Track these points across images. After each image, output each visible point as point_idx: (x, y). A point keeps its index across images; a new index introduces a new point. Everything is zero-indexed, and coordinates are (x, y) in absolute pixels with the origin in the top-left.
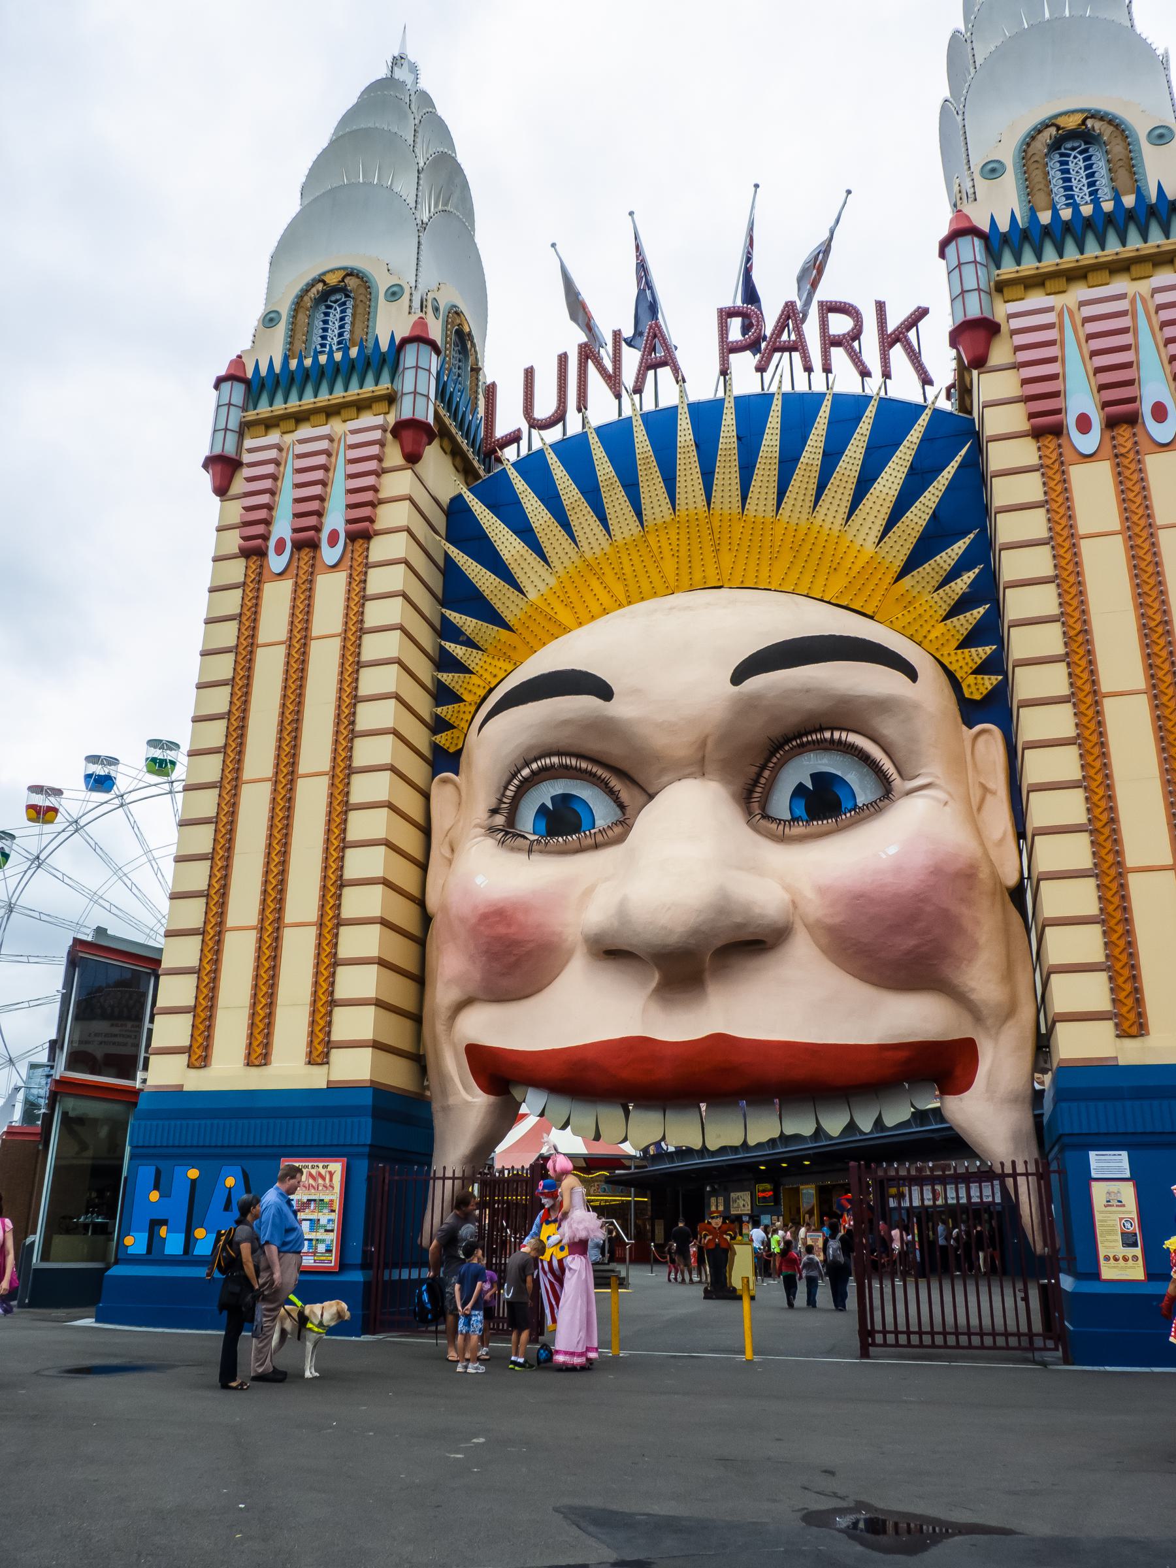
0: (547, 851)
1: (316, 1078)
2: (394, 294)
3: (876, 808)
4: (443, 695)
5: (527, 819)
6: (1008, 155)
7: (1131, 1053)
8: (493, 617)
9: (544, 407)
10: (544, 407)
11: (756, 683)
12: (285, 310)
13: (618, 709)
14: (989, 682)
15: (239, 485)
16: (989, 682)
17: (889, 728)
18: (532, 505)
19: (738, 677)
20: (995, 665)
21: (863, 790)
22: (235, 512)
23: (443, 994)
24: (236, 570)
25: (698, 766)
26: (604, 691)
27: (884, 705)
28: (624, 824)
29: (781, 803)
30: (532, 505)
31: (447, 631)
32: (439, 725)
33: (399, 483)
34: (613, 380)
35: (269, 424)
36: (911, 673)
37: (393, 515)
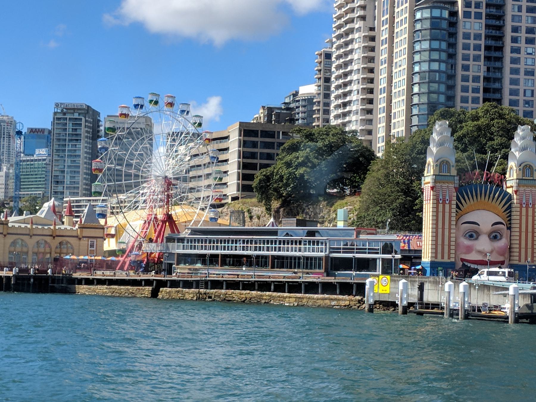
0: (470, 240)
1: (449, 261)
3: (500, 239)
5: (467, 235)
7: (520, 263)
11: (494, 226)
12: (438, 164)
14: (510, 225)
16: (510, 225)
17: (502, 231)
18: (466, 196)
19: (492, 225)
20: (510, 224)
22: (435, 193)
23: (458, 253)
24: (435, 201)
25: (486, 234)
26: (479, 225)
27: (503, 229)
29: (491, 237)
30: (466, 196)
36: (505, 225)
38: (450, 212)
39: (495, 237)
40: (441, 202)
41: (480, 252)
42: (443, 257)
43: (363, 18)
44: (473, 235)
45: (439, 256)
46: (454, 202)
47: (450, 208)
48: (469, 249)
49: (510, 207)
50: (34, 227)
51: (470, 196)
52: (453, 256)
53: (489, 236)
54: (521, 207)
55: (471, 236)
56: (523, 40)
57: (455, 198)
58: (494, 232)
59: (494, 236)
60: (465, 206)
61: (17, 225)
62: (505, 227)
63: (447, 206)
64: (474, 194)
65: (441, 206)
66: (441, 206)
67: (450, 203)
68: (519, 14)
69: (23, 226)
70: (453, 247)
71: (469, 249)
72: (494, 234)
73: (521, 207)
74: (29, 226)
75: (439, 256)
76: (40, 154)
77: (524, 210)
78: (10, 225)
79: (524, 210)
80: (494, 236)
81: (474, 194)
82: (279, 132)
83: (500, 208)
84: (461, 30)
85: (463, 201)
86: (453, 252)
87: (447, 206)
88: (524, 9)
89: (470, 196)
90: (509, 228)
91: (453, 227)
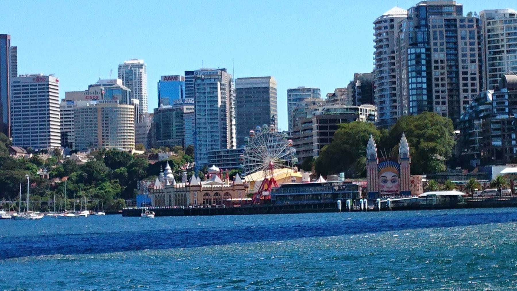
39: (394, 182)
41: (388, 188)
42: (373, 190)
43: (388, 46)
44: (385, 181)
45: (372, 190)
46: (377, 169)
47: (375, 172)
48: (383, 187)
49: (399, 169)
50: (213, 186)
52: (377, 190)
54: (403, 169)
56: (469, 61)
58: (394, 179)
59: (393, 181)
60: (382, 170)
61: (206, 186)
62: (398, 178)
63: (374, 171)
68: (466, 47)
69: (208, 186)
70: (377, 187)
71: (383, 187)
73: (403, 169)
74: (211, 186)
75: (372, 190)
76: (178, 104)
78: (203, 186)
79: (404, 170)
80: (393, 181)
82: (339, 120)
83: (396, 170)
84: (433, 58)
86: (377, 188)
87: (374, 171)
88: (468, 44)
90: (400, 177)
91: (377, 179)
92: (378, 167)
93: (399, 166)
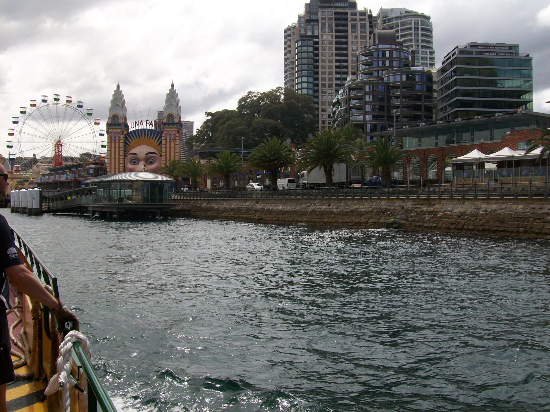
2: (120, 118)
4: (125, 151)
6: (166, 116)
8: (129, 145)
9: (132, 127)
10: (132, 127)
13: (138, 156)
15: (109, 133)
19: (146, 155)
21: (153, 162)
24: (109, 141)
25: (142, 160)
28: (138, 163)
31: (125, 146)
32: (125, 153)
33: (122, 136)
34: (138, 125)
35: (110, 129)
37: (122, 138)
38: (119, 148)
39: (151, 163)
40: (113, 141)
47: (119, 145)
49: (161, 142)
51: (135, 136)
53: (147, 162)
54: (166, 142)
55: (134, 162)
57: (122, 138)
62: (158, 156)
63: (117, 144)
64: (137, 135)
65: (113, 144)
66: (113, 144)
67: (119, 143)
72: (150, 161)
73: (166, 142)
77: (168, 143)
79: (168, 143)
81: (137, 135)
83: (155, 143)
85: (130, 140)
87: (117, 144)
89: (135, 136)
92: (126, 138)
93: (161, 137)
